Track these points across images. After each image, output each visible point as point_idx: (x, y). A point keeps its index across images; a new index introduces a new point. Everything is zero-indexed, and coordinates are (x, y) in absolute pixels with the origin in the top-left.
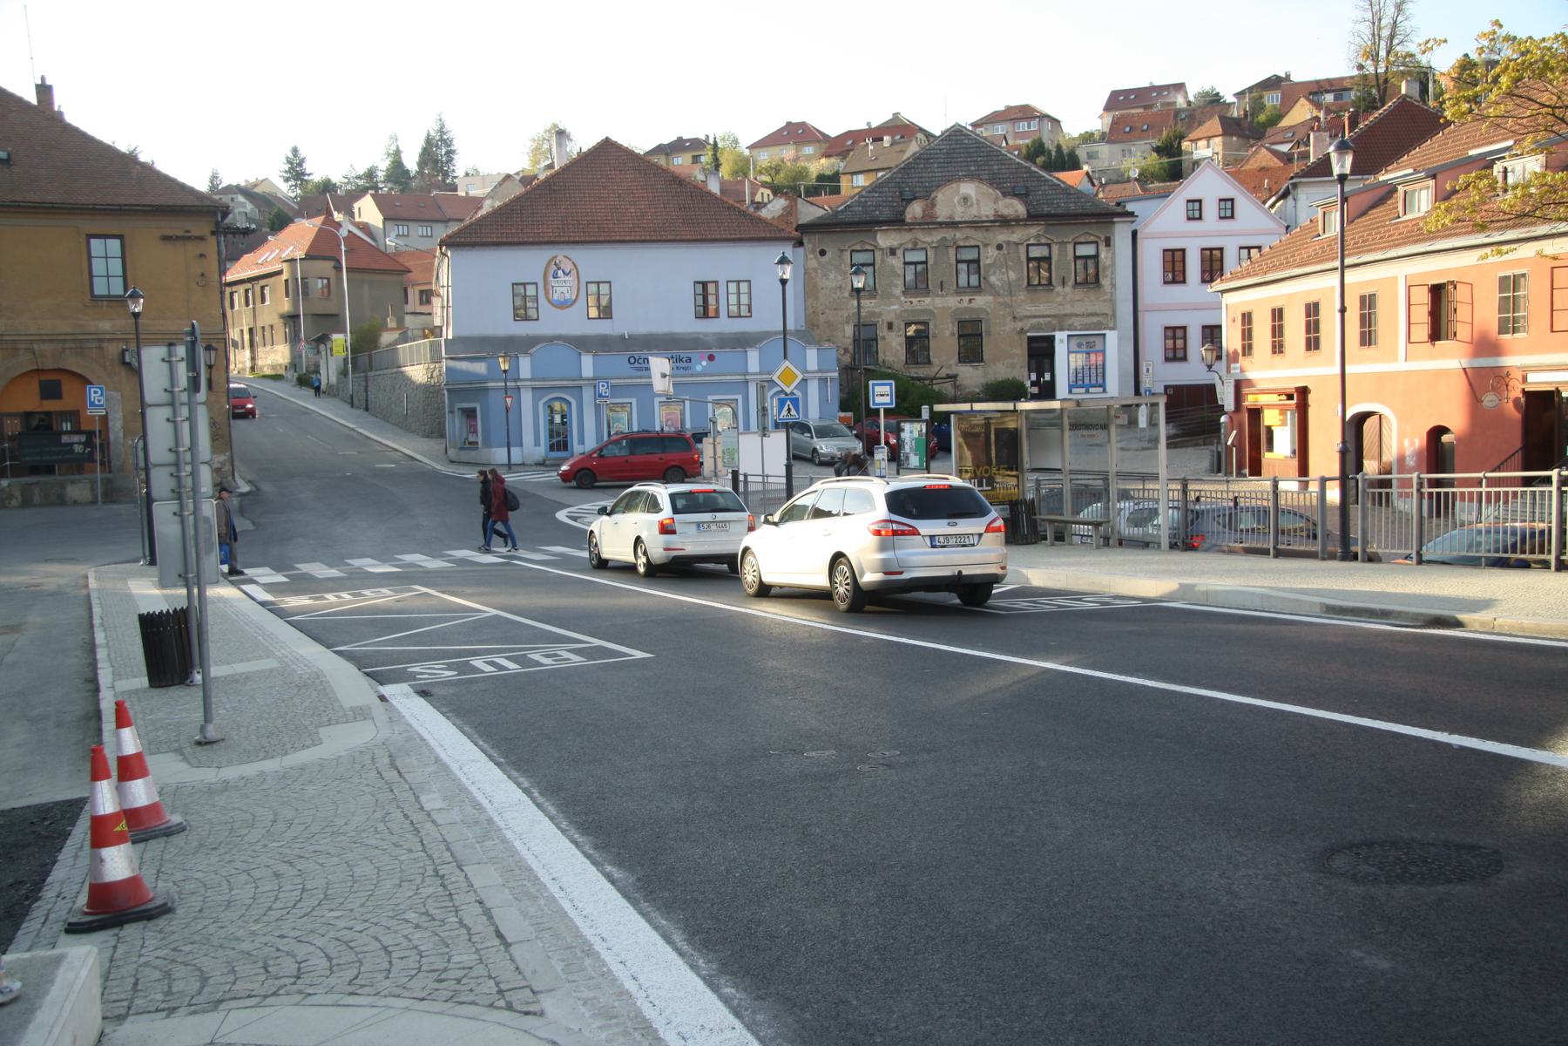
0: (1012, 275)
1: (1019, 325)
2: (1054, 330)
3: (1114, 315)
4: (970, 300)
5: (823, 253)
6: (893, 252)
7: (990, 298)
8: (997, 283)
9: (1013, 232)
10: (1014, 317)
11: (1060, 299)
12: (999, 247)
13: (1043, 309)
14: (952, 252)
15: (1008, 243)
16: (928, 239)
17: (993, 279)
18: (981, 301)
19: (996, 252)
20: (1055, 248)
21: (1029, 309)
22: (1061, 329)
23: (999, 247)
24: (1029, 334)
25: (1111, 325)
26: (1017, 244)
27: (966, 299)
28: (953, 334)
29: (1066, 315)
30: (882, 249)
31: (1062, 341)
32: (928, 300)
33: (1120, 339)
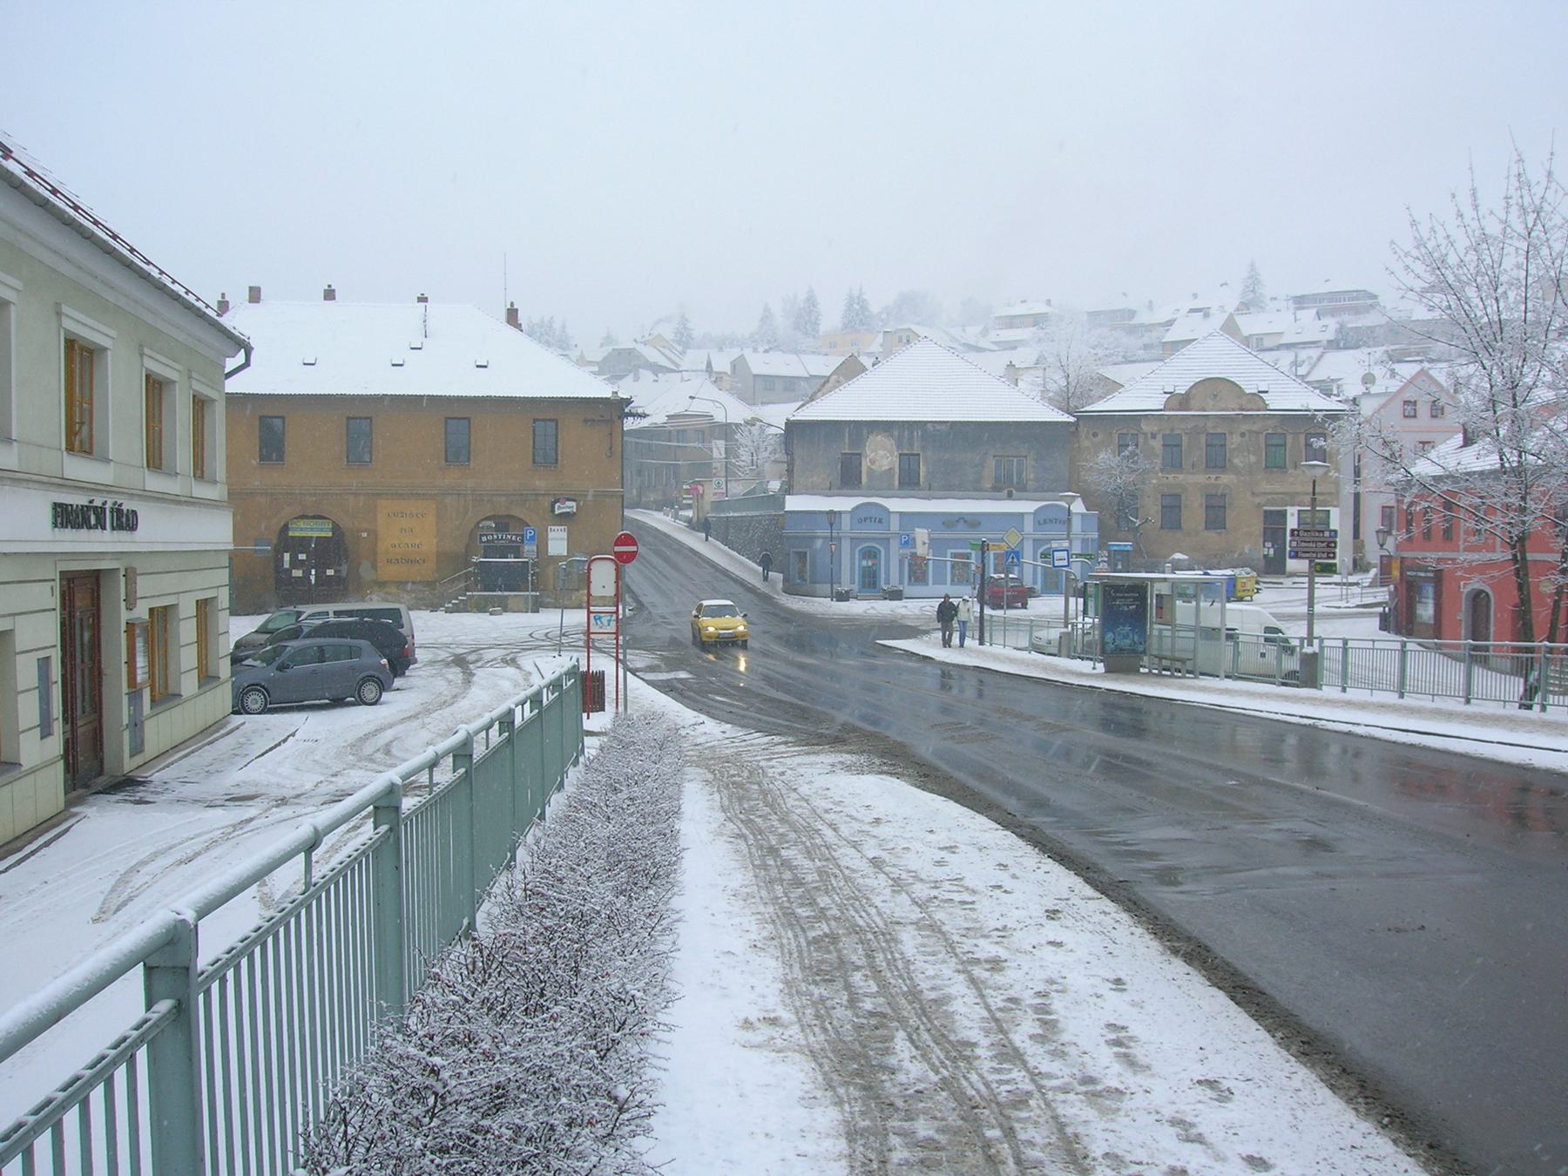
0: (1253, 458)
1: (1258, 500)
2: (1286, 505)
3: (1338, 493)
4: (1217, 478)
5: (1095, 435)
6: (1154, 436)
7: (1232, 477)
8: (1241, 465)
9: (1254, 423)
10: (1253, 493)
11: (1292, 479)
12: (1243, 435)
13: (1278, 488)
14: (1203, 438)
15: (1250, 431)
16: (1183, 426)
17: (1236, 461)
18: (1226, 479)
19: (1239, 439)
20: (1289, 438)
21: (1266, 487)
22: (1292, 505)
23: (1243, 435)
24: (1265, 508)
25: (1335, 503)
26: (1257, 433)
27: (1213, 476)
28: (1201, 505)
29: (1297, 493)
30: (1145, 434)
31: (1292, 515)
32: (1181, 477)
33: (1342, 515)
